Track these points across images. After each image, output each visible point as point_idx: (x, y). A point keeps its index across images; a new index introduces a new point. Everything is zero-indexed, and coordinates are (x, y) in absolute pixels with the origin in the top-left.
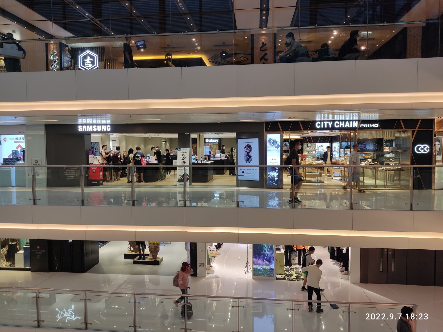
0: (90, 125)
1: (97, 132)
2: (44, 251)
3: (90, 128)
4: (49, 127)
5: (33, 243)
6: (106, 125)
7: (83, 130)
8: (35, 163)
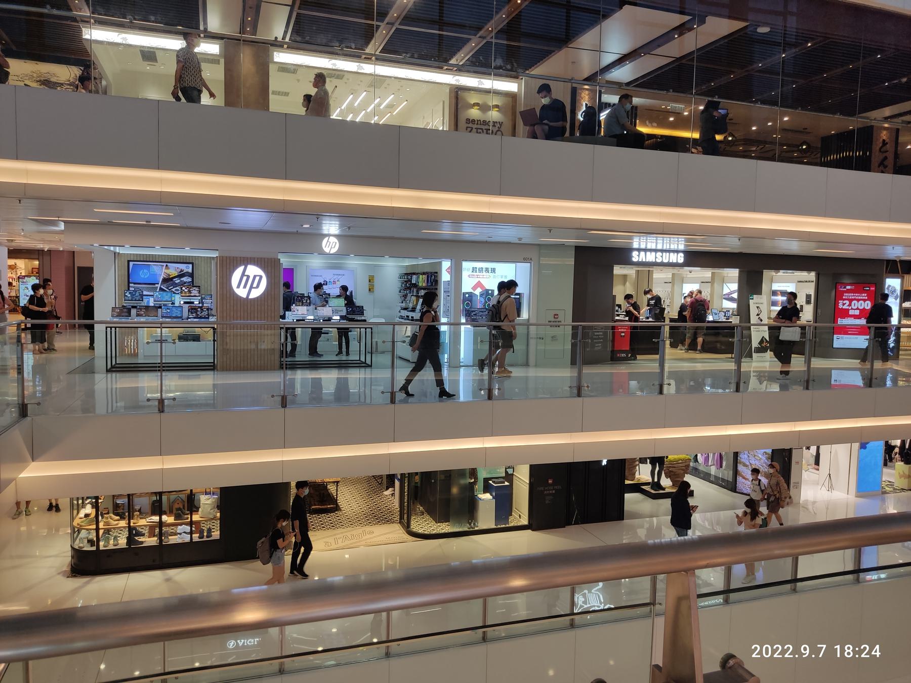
0: (651, 250)
1: (662, 264)
2: (559, 487)
3: (651, 257)
4: (581, 252)
5: (539, 473)
6: (677, 252)
7: (640, 260)
8: (553, 319)
